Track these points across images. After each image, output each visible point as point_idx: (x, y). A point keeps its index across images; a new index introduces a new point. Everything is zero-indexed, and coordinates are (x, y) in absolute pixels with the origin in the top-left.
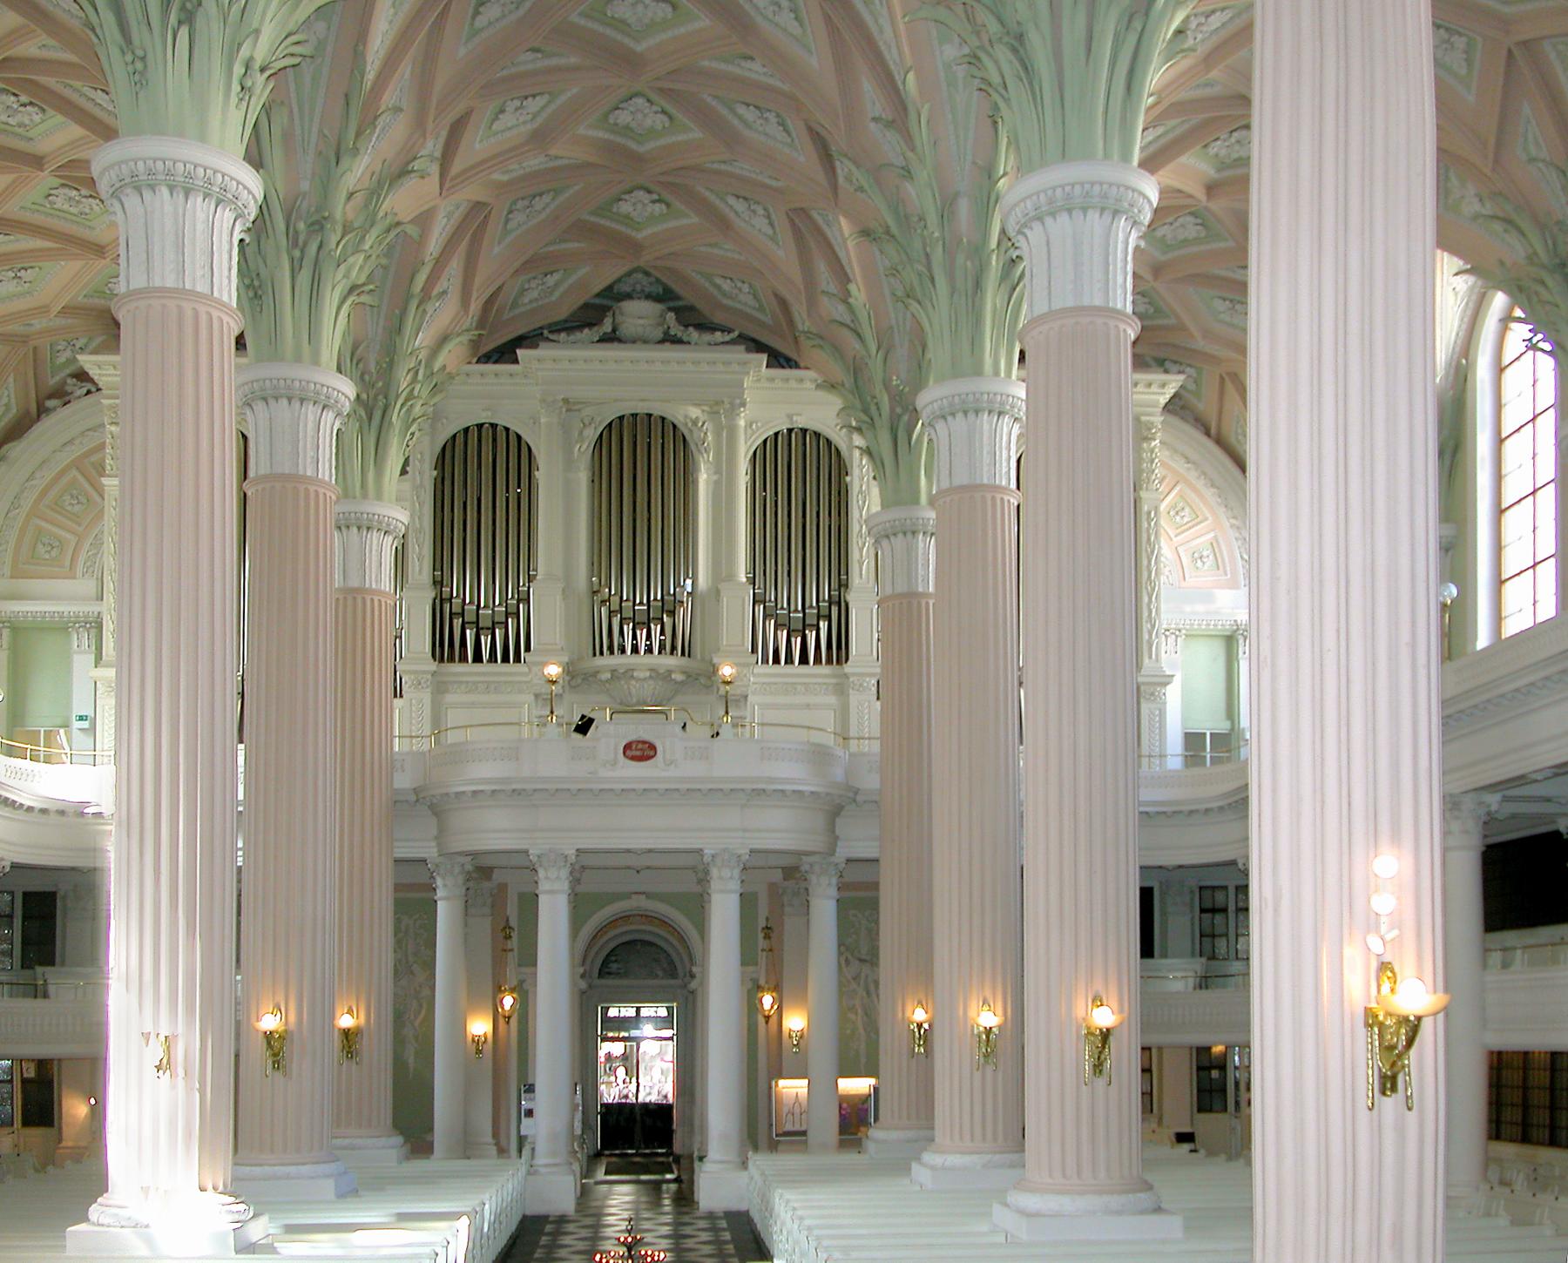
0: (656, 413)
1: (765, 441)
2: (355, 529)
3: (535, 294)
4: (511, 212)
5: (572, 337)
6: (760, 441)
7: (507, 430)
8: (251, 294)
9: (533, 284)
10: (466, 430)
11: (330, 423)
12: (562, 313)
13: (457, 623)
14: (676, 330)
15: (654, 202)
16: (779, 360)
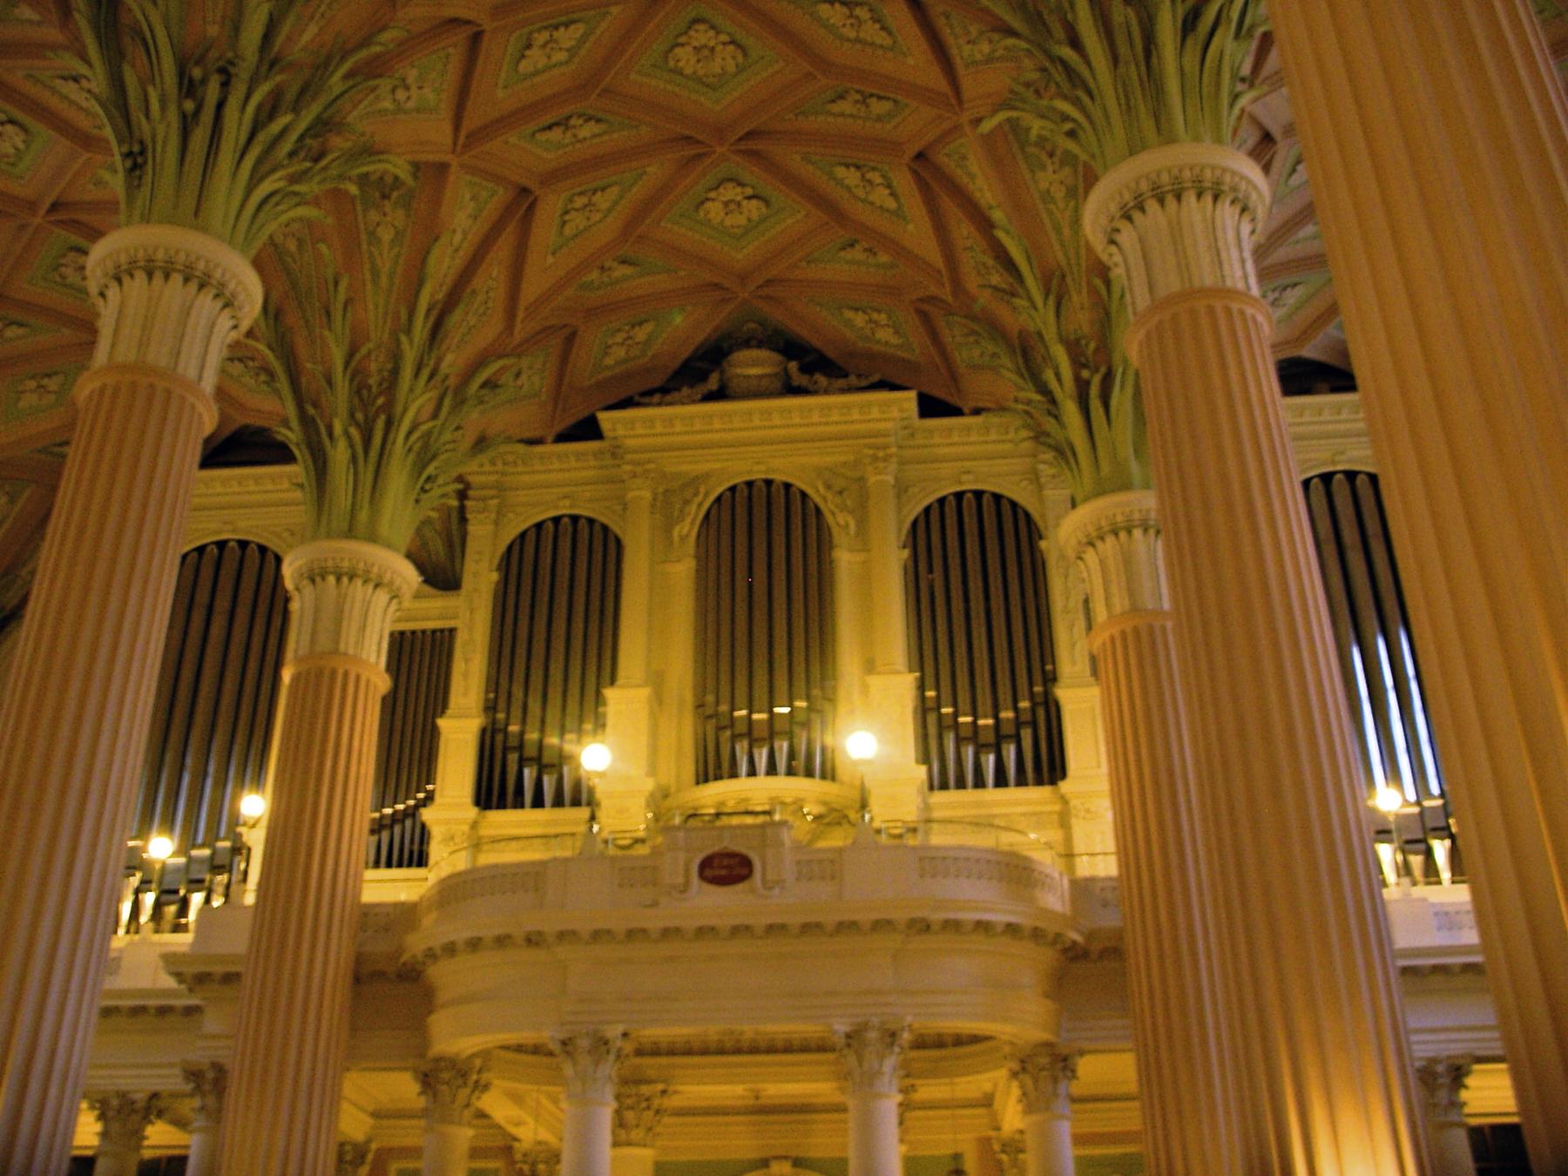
0: (779, 477)
1: (927, 510)
2: (331, 579)
3: (621, 353)
4: (567, 212)
5: (668, 398)
6: (919, 508)
7: (591, 521)
8: (129, 163)
9: (619, 338)
10: (539, 526)
11: (225, 332)
12: (657, 380)
13: (513, 758)
14: (799, 379)
15: (749, 198)
16: (931, 407)
